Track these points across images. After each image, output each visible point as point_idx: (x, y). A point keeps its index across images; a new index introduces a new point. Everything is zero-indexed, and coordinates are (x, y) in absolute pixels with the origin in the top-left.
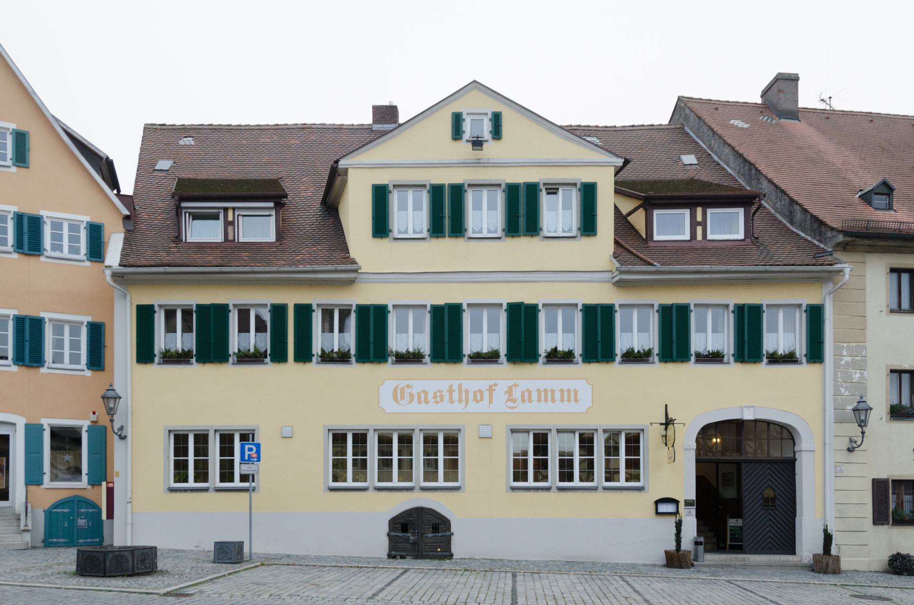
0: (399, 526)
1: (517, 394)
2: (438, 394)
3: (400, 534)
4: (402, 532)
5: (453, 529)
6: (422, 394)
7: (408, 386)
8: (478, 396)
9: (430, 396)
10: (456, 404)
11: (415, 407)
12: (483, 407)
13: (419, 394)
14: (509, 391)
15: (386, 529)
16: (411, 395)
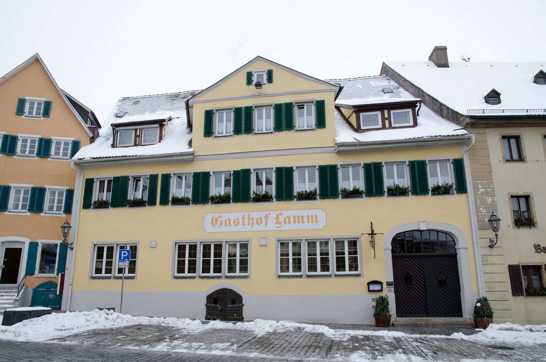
0: (212, 300)
1: (281, 219)
2: (237, 221)
3: (213, 305)
4: (214, 303)
5: (244, 302)
6: (228, 221)
7: (220, 217)
8: (259, 221)
9: (232, 222)
10: (247, 226)
11: (223, 229)
12: (262, 227)
13: (226, 221)
14: (277, 218)
15: (205, 301)
16: (221, 222)
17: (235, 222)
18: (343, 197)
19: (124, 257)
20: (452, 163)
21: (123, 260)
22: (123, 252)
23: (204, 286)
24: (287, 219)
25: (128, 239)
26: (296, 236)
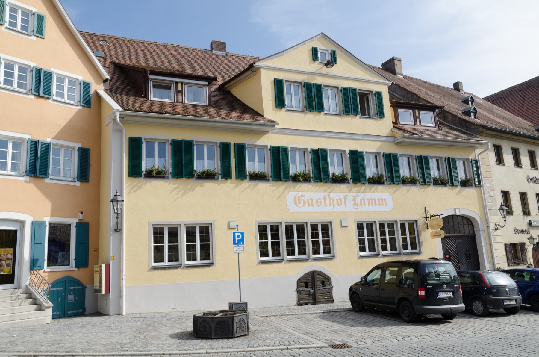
0: (303, 284)
1: (358, 201)
2: (319, 201)
3: (305, 289)
4: (306, 287)
5: (333, 283)
6: (310, 201)
7: (302, 196)
8: (339, 203)
9: (314, 202)
10: (328, 206)
11: (306, 209)
12: (341, 209)
13: (308, 201)
14: (354, 200)
15: (295, 287)
16: (304, 201)
17: (317, 202)
18: (144, 178)
19: (238, 240)
20: (219, 147)
21: (238, 244)
22: (236, 234)
23: (293, 270)
24: (310, 201)
25: (198, 218)
26: (300, 219)
